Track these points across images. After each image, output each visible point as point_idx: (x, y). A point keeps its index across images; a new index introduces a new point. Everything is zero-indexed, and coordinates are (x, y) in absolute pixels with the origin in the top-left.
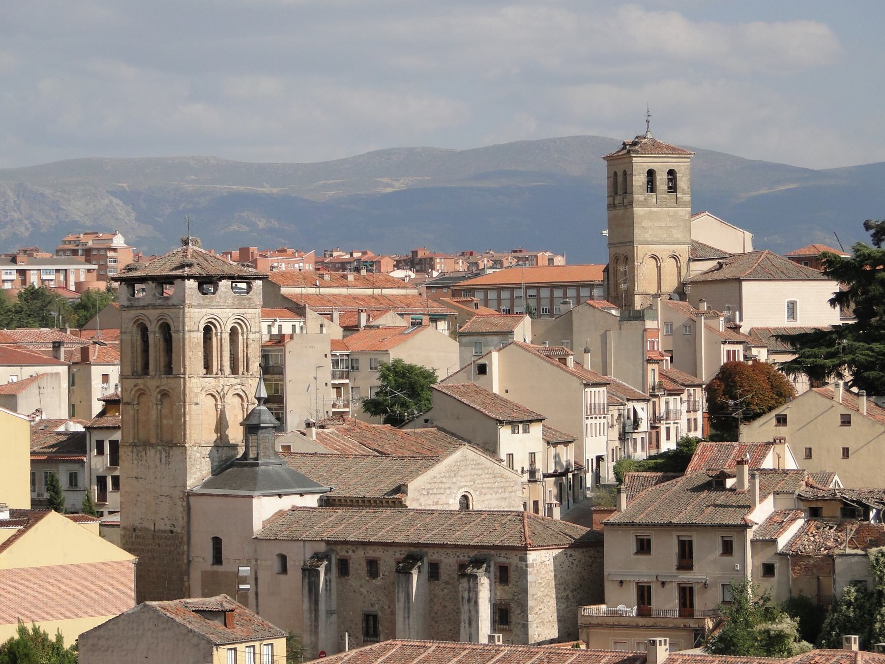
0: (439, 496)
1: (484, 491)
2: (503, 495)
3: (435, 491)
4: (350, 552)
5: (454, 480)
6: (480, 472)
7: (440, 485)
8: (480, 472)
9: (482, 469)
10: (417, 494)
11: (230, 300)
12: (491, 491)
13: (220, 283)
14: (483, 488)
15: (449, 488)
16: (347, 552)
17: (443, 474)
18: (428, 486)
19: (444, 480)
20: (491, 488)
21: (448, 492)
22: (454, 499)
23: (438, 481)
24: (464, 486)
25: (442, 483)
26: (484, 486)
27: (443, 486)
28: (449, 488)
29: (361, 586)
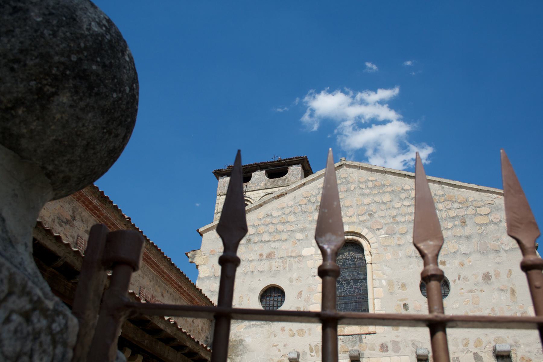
0: (276, 245)
3: (266, 237)
6: (386, 198)
7: (280, 227)
8: (386, 198)
9: (389, 192)
13: (253, 174)
14: (397, 223)
17: (288, 211)
19: (291, 218)
21: (299, 236)
26: (400, 219)
27: (288, 227)
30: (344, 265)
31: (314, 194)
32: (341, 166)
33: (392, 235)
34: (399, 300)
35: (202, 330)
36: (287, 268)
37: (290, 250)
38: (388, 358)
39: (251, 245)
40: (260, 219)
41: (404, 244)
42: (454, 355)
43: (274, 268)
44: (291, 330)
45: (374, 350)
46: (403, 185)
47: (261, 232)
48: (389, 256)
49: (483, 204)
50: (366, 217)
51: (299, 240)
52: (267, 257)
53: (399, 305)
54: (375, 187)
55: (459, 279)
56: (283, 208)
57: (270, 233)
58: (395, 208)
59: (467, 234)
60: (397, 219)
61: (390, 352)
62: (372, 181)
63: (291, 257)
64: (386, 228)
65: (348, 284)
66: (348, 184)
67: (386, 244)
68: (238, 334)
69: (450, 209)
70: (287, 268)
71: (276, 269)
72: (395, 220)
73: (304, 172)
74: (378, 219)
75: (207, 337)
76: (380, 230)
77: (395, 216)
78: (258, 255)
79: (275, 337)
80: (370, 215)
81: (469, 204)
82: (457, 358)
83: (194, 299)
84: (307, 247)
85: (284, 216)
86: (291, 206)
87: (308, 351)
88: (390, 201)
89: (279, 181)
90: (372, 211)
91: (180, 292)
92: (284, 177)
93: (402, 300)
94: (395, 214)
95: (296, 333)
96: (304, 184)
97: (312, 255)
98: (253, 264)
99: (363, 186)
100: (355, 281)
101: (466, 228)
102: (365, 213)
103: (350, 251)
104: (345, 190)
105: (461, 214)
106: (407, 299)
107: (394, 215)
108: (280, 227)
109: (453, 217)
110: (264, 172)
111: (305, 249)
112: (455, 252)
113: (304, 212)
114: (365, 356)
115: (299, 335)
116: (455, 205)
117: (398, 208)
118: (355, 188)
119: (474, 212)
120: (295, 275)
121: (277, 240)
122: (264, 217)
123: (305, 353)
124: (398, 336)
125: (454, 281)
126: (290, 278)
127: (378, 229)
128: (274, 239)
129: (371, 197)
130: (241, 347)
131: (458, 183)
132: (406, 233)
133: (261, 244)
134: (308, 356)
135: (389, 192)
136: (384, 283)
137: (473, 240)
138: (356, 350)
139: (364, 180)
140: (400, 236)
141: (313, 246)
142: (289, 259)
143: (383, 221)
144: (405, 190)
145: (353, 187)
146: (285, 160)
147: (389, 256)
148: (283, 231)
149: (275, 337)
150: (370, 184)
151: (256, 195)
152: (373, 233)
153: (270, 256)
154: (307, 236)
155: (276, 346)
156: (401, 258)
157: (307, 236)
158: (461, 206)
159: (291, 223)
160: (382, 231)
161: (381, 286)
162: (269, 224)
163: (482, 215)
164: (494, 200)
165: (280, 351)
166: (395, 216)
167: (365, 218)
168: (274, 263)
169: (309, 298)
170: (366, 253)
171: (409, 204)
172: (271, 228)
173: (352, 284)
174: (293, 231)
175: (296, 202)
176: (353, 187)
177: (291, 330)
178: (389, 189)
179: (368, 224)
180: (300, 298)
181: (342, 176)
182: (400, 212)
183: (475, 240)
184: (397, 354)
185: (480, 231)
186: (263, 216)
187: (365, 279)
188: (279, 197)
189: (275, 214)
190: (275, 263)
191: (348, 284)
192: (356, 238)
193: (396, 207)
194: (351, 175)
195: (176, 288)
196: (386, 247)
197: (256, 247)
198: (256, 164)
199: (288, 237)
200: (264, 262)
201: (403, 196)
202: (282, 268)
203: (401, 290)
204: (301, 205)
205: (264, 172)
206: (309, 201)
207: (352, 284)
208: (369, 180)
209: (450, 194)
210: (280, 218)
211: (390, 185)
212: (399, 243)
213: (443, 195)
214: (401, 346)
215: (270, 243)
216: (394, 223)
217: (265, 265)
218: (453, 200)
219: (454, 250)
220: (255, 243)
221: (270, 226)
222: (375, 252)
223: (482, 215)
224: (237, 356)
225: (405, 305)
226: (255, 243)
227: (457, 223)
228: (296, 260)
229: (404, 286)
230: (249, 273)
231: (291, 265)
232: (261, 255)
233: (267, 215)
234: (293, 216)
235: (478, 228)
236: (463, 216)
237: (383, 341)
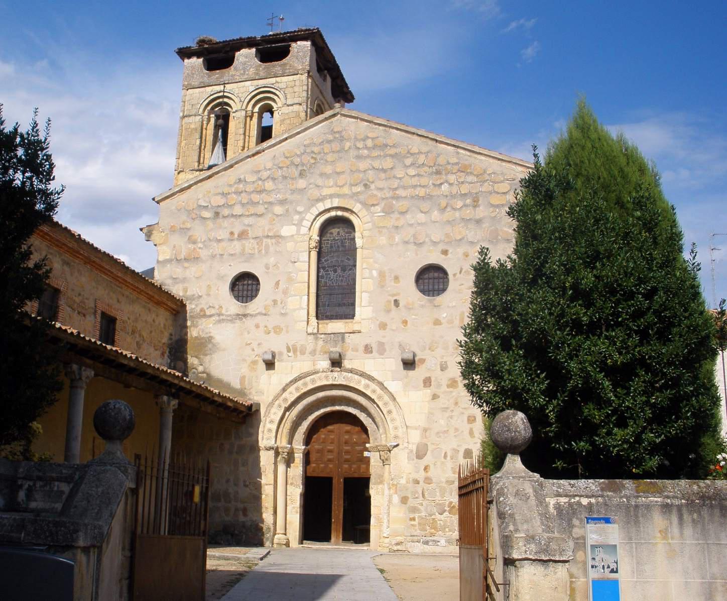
1: (399, 205)
2: (468, 213)
3: (238, 210)
5: (302, 183)
6: (388, 163)
7: (256, 197)
8: (388, 163)
9: (392, 156)
10: (184, 217)
12: (425, 206)
13: (237, 54)
14: (398, 198)
15: (282, 202)
17: (265, 174)
18: (220, 201)
19: (269, 185)
20: (428, 197)
21: (278, 210)
22: (299, 224)
23: (250, 188)
24: (331, 196)
25: (260, 192)
27: (264, 197)
28: (282, 202)
30: (331, 247)
31: (298, 153)
32: (334, 115)
33: (389, 214)
34: (390, 295)
35: (165, 328)
36: (263, 251)
37: (266, 229)
38: (372, 361)
39: (220, 220)
40: (230, 186)
41: (402, 226)
42: (442, 358)
43: (248, 250)
44: (266, 327)
45: (357, 351)
46: (410, 147)
47: (232, 203)
48: (383, 240)
49: (502, 179)
50: (359, 188)
51: (278, 216)
52: (238, 236)
53: (389, 301)
54: (375, 147)
55: (460, 272)
56: (259, 171)
57: (243, 205)
58: (397, 178)
59: (477, 217)
60: (397, 192)
61: (375, 354)
62: (373, 139)
63: (268, 237)
64: (383, 204)
65: (335, 271)
66: (341, 141)
67: (381, 225)
68: (207, 331)
69: (463, 183)
70: (263, 251)
71: (250, 252)
72: (395, 194)
73: (316, 50)
74: (375, 192)
75: (171, 335)
76: (377, 207)
77: (396, 189)
78: (228, 233)
79: (249, 333)
80: (366, 185)
81: (487, 177)
82: (446, 362)
83: (153, 297)
84: (287, 225)
85: (260, 182)
86: (269, 169)
87: (285, 351)
88: (392, 168)
89: (276, 66)
90: (368, 180)
91: (138, 292)
92: (284, 61)
93: (393, 295)
94: (396, 186)
95: (272, 331)
96: (286, 139)
97: (292, 236)
98: (223, 244)
99: (360, 145)
100: (344, 270)
101: (477, 209)
102: (360, 183)
103: (339, 228)
104: (338, 149)
105: (474, 191)
106: (398, 294)
107: (394, 187)
108: (256, 197)
109: (465, 195)
110: (254, 50)
111: (284, 227)
112: (460, 240)
113: (285, 178)
114: (347, 358)
115: (275, 332)
116: (470, 178)
117: (400, 179)
118: (350, 148)
119: (490, 188)
120: (272, 260)
121: (251, 215)
122: (235, 183)
123: (281, 354)
124: (384, 337)
125: (454, 275)
126: (267, 264)
127: (373, 205)
128: (247, 213)
129: (369, 161)
130: (210, 346)
131: (477, 149)
132: (406, 212)
133: (232, 219)
134: (285, 357)
135: (392, 156)
136: (375, 273)
137: (484, 226)
138: (336, 352)
139: (362, 137)
140: (398, 216)
141: (294, 224)
142: (265, 240)
143: (379, 194)
144: (412, 154)
145: (347, 145)
146: (285, 33)
147: (383, 240)
148: (258, 203)
149: (249, 333)
150: (369, 143)
151: (242, 90)
152: (367, 210)
153: (243, 235)
154: (287, 211)
155: (249, 344)
156: (397, 244)
157: (287, 211)
158: (475, 179)
159: (268, 192)
160: (378, 208)
161: (371, 277)
162: (242, 192)
163: (498, 193)
164: (517, 174)
165: (253, 350)
166: (396, 189)
167: (359, 190)
168: (247, 245)
169: (287, 288)
170: (357, 235)
171: (414, 173)
172: (244, 198)
173: (339, 271)
174: (270, 203)
175: (276, 163)
176: (347, 145)
177: (266, 327)
178: (392, 151)
179: (362, 197)
180: (277, 288)
181: (335, 130)
182: (402, 184)
183: (485, 225)
184: (382, 356)
185: (493, 215)
186: (234, 181)
187: (355, 266)
188: (254, 155)
189: (251, 178)
190: (249, 245)
191: (335, 271)
192: (346, 214)
193: (398, 176)
194: (347, 128)
195: (132, 289)
196: (380, 229)
197: (225, 223)
198: (241, 39)
199: (264, 211)
200: (236, 243)
201: (408, 161)
202: (256, 250)
203: (393, 283)
204: (281, 168)
205: (254, 50)
206: (292, 163)
207: (339, 271)
208: (368, 137)
209: (466, 163)
210: (255, 185)
211: (394, 146)
212: (396, 225)
213: (457, 164)
214: (387, 347)
215: (242, 218)
216: (393, 198)
217: (236, 246)
218: (469, 171)
219: (459, 237)
220: (224, 217)
221: (243, 195)
222: (367, 235)
223: (498, 193)
224: (206, 355)
225: (396, 301)
226: (224, 217)
227: (468, 201)
228: (274, 241)
229: (396, 278)
230: (218, 256)
231: (267, 247)
232: (232, 233)
233: (240, 180)
234: (271, 183)
235: (491, 209)
236: (476, 193)
237: (367, 341)
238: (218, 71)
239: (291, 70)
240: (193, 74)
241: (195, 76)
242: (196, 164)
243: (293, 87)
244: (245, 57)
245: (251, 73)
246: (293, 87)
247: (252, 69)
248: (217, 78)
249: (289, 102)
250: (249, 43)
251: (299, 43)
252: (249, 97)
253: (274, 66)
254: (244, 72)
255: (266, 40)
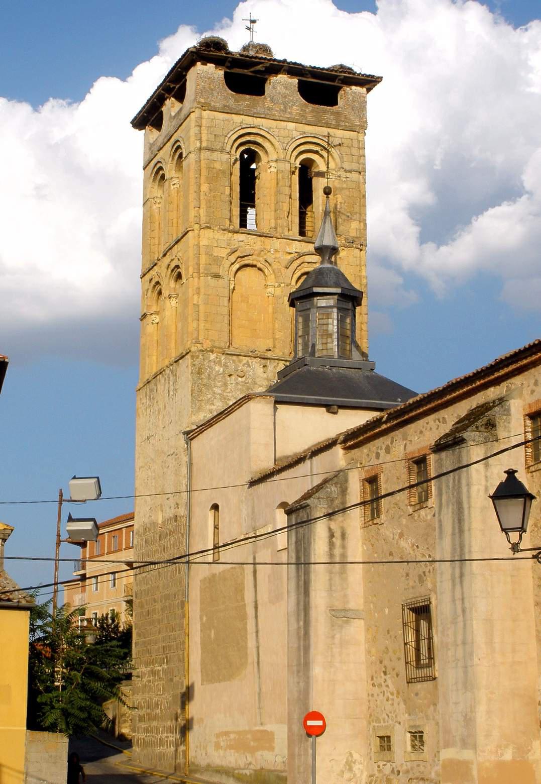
4: (382, 453)
11: (295, 110)
16: (378, 456)
29: (401, 535)
110: (295, 81)
198: (285, 61)
205: (295, 81)
238: (248, 96)
239: (347, 124)
240: (212, 90)
241: (216, 94)
242: (228, 222)
243: (350, 147)
244: (281, 86)
245: (294, 113)
246: (350, 147)
247: (295, 107)
248: (247, 106)
249: (347, 166)
250: (294, 70)
251: (354, 88)
252: (294, 145)
253: (325, 112)
254: (285, 107)
255: (315, 72)
